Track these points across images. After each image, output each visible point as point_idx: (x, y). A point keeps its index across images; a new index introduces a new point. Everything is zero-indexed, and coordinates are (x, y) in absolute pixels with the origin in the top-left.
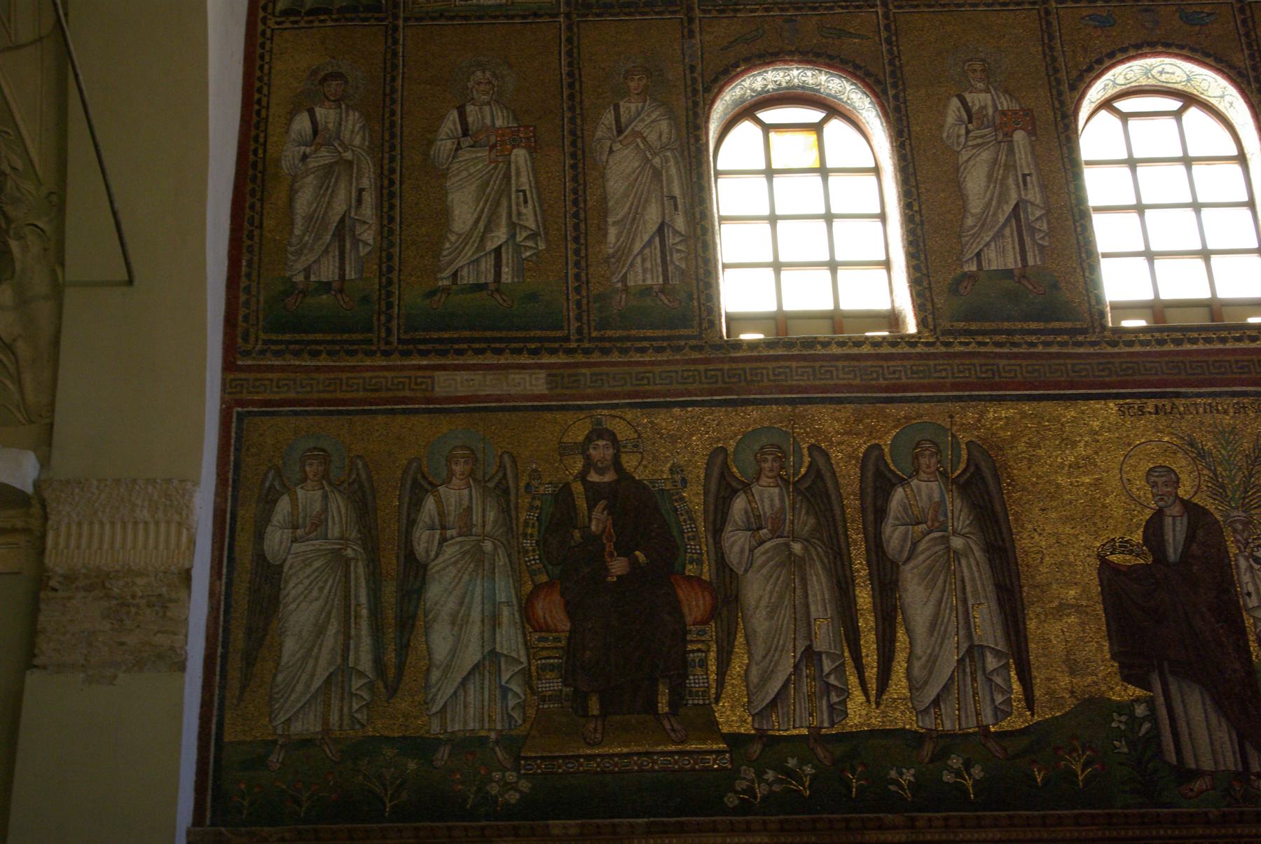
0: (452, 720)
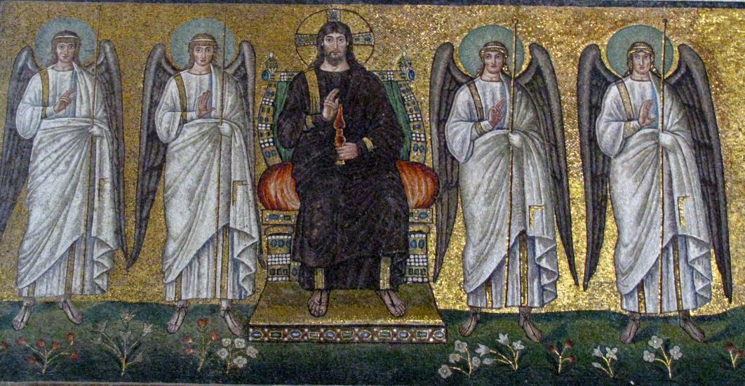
0: (187, 288)
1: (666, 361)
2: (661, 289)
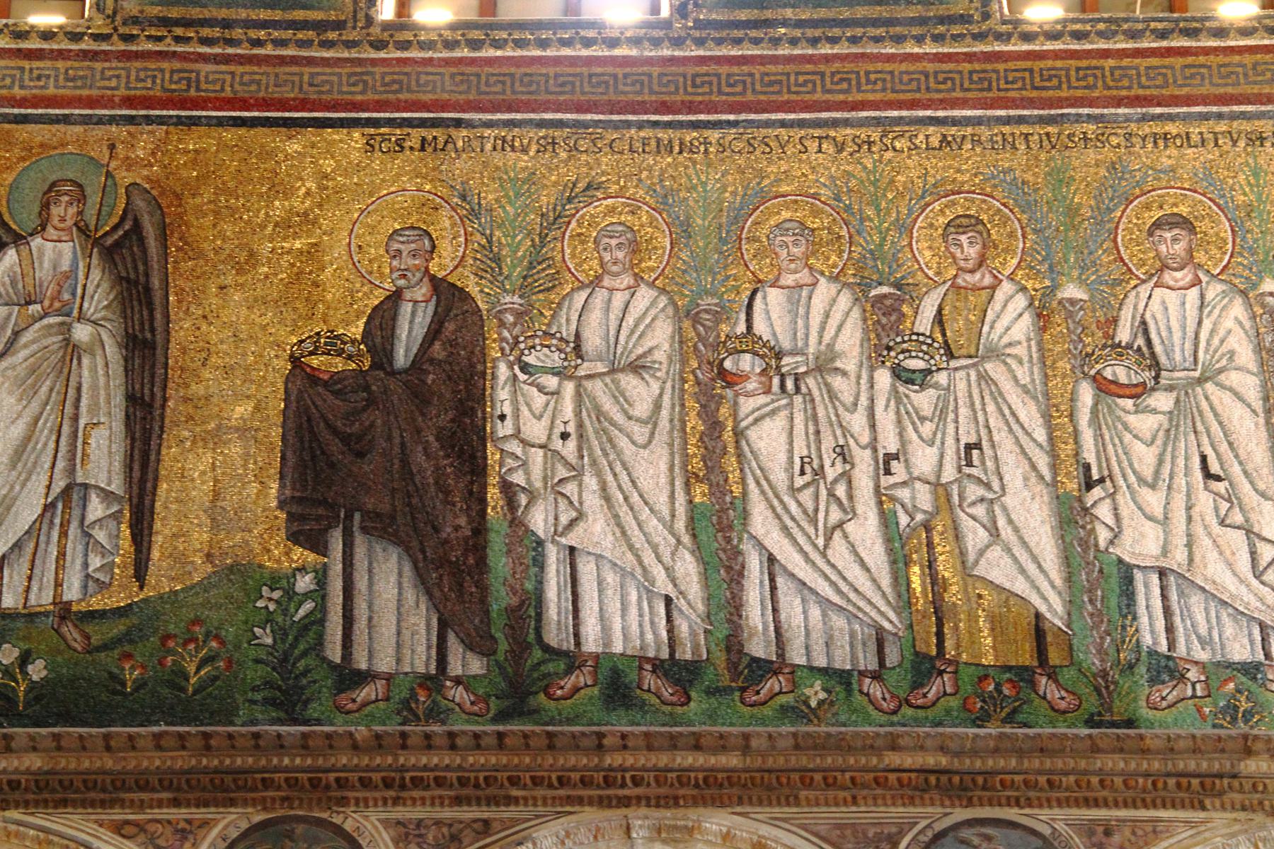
1: (17, 683)
2: (31, 570)
